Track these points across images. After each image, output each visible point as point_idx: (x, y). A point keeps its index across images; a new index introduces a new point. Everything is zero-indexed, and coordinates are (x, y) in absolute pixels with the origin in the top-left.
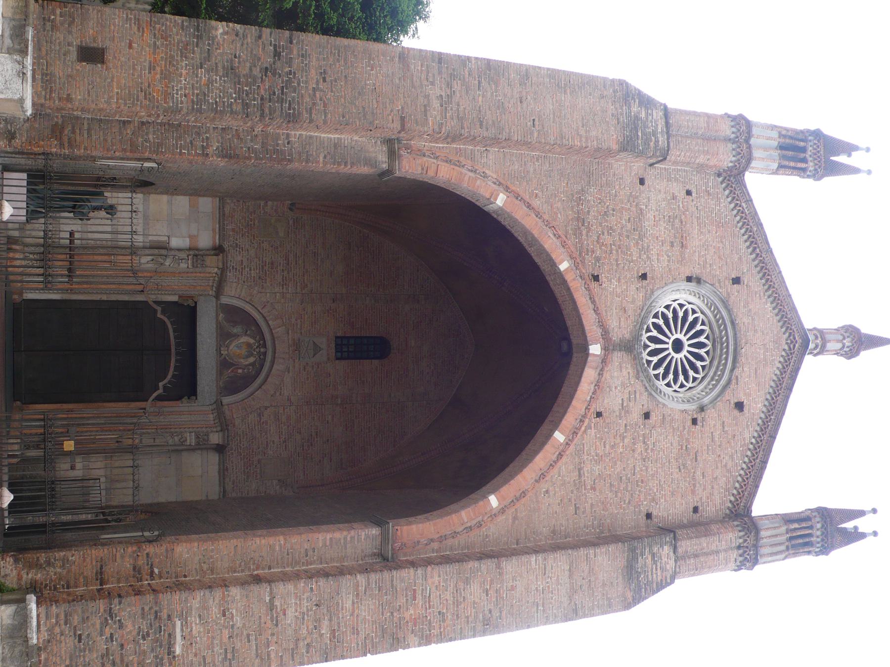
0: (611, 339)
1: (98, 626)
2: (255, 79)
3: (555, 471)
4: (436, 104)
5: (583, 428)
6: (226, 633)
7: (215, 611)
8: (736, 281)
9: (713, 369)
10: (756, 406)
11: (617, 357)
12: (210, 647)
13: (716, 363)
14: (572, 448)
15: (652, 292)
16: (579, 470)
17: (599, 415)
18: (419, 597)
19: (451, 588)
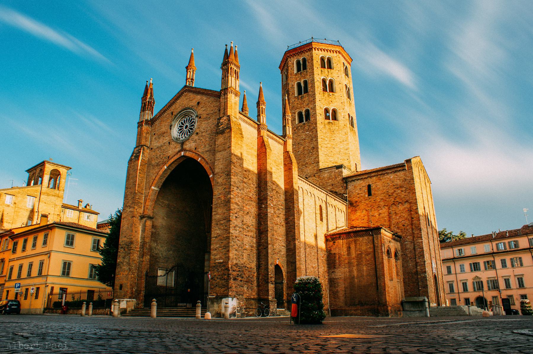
0: (181, 150)
1: (214, 281)
2: (126, 252)
3: (206, 159)
4: (131, 209)
5: (198, 153)
6: (220, 249)
7: (215, 252)
8: (172, 113)
9: (192, 114)
10: (198, 97)
11: (185, 147)
12: (222, 252)
13: (190, 114)
14: (202, 155)
15: (173, 140)
16: (207, 151)
17: (196, 148)
18: (220, 196)
19: (219, 187)
